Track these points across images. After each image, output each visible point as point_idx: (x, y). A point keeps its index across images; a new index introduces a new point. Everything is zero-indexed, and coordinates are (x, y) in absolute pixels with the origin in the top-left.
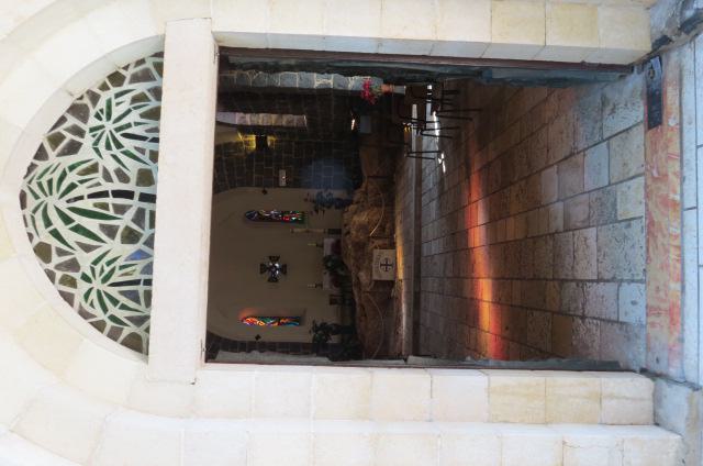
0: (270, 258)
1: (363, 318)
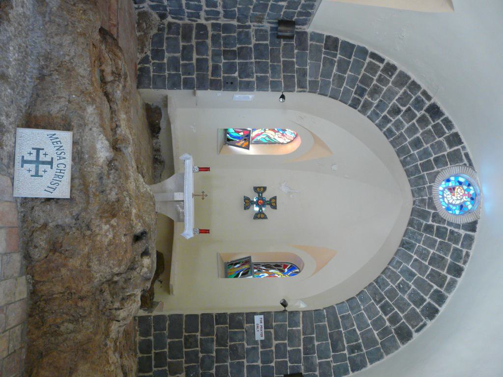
0: (265, 217)
1: (109, 78)
